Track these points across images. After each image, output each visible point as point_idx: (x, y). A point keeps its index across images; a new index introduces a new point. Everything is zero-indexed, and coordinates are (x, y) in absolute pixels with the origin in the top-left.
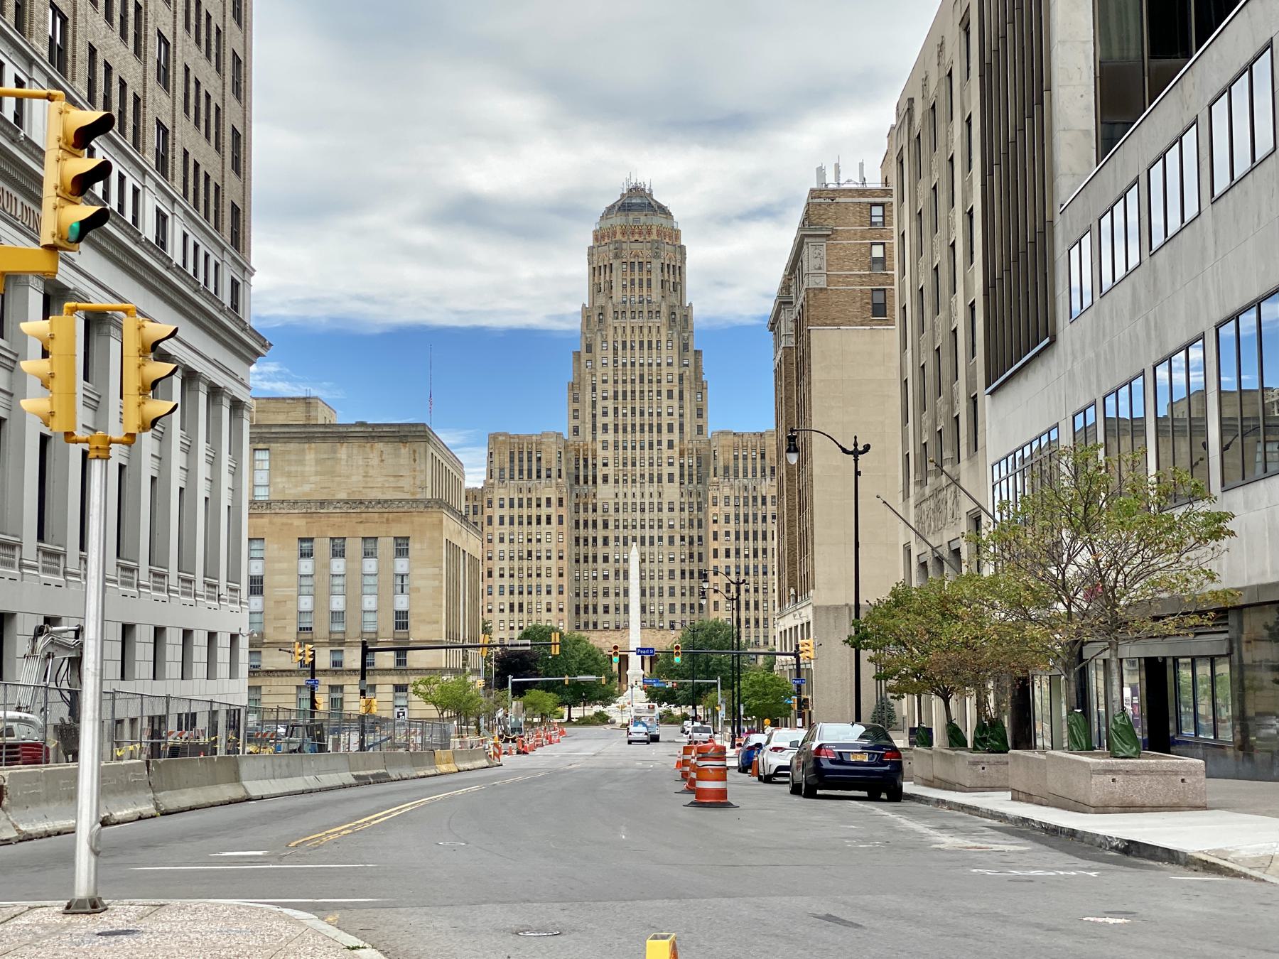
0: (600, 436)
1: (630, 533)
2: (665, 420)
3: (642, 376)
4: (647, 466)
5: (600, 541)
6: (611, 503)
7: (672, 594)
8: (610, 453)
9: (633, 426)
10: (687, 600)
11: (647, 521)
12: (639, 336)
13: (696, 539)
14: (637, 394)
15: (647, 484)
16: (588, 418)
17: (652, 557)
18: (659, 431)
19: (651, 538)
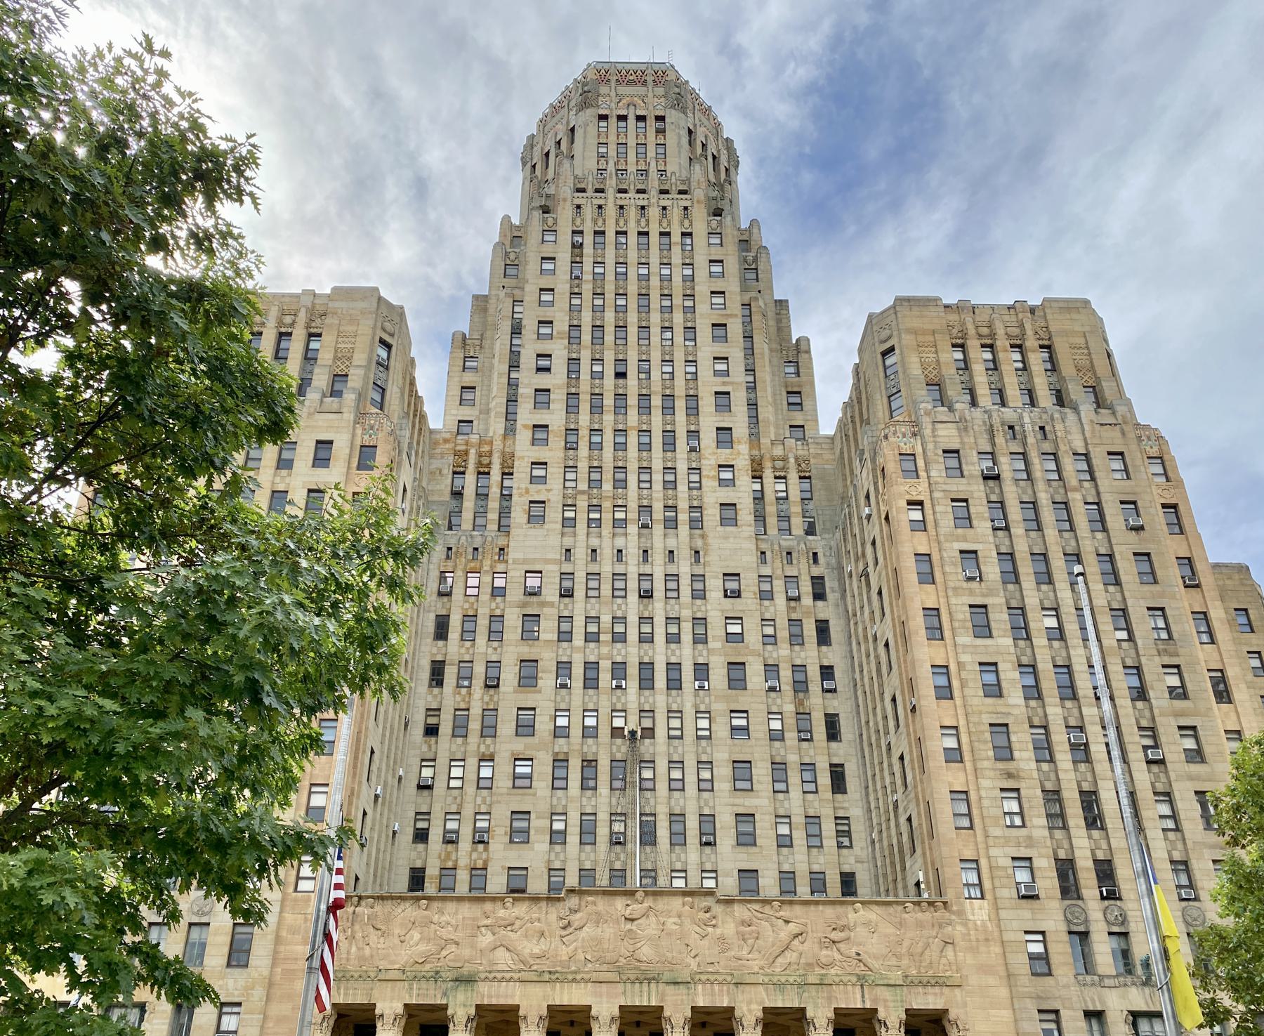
0: (526, 415)
1: (605, 653)
2: (708, 386)
3: (645, 296)
4: (658, 486)
5: (509, 676)
6: (552, 572)
7: (746, 839)
8: (553, 453)
9: (621, 397)
10: (799, 860)
11: (659, 621)
12: (639, 221)
13: (814, 673)
14: (633, 331)
15: (658, 529)
16: (498, 403)
17: (675, 723)
18: (693, 410)
19: (674, 668)
